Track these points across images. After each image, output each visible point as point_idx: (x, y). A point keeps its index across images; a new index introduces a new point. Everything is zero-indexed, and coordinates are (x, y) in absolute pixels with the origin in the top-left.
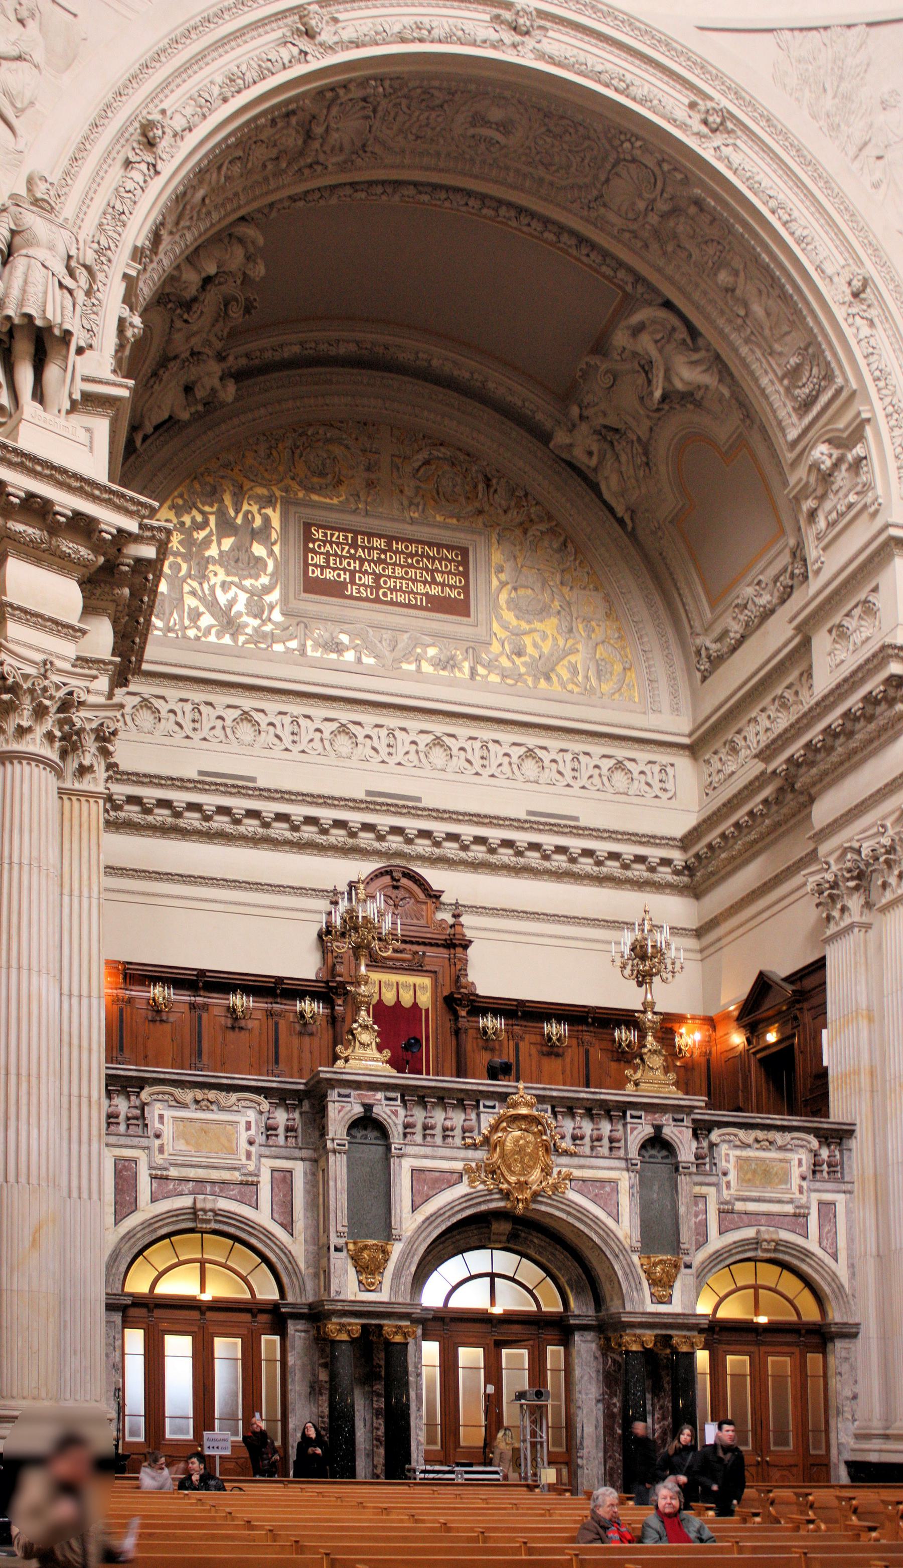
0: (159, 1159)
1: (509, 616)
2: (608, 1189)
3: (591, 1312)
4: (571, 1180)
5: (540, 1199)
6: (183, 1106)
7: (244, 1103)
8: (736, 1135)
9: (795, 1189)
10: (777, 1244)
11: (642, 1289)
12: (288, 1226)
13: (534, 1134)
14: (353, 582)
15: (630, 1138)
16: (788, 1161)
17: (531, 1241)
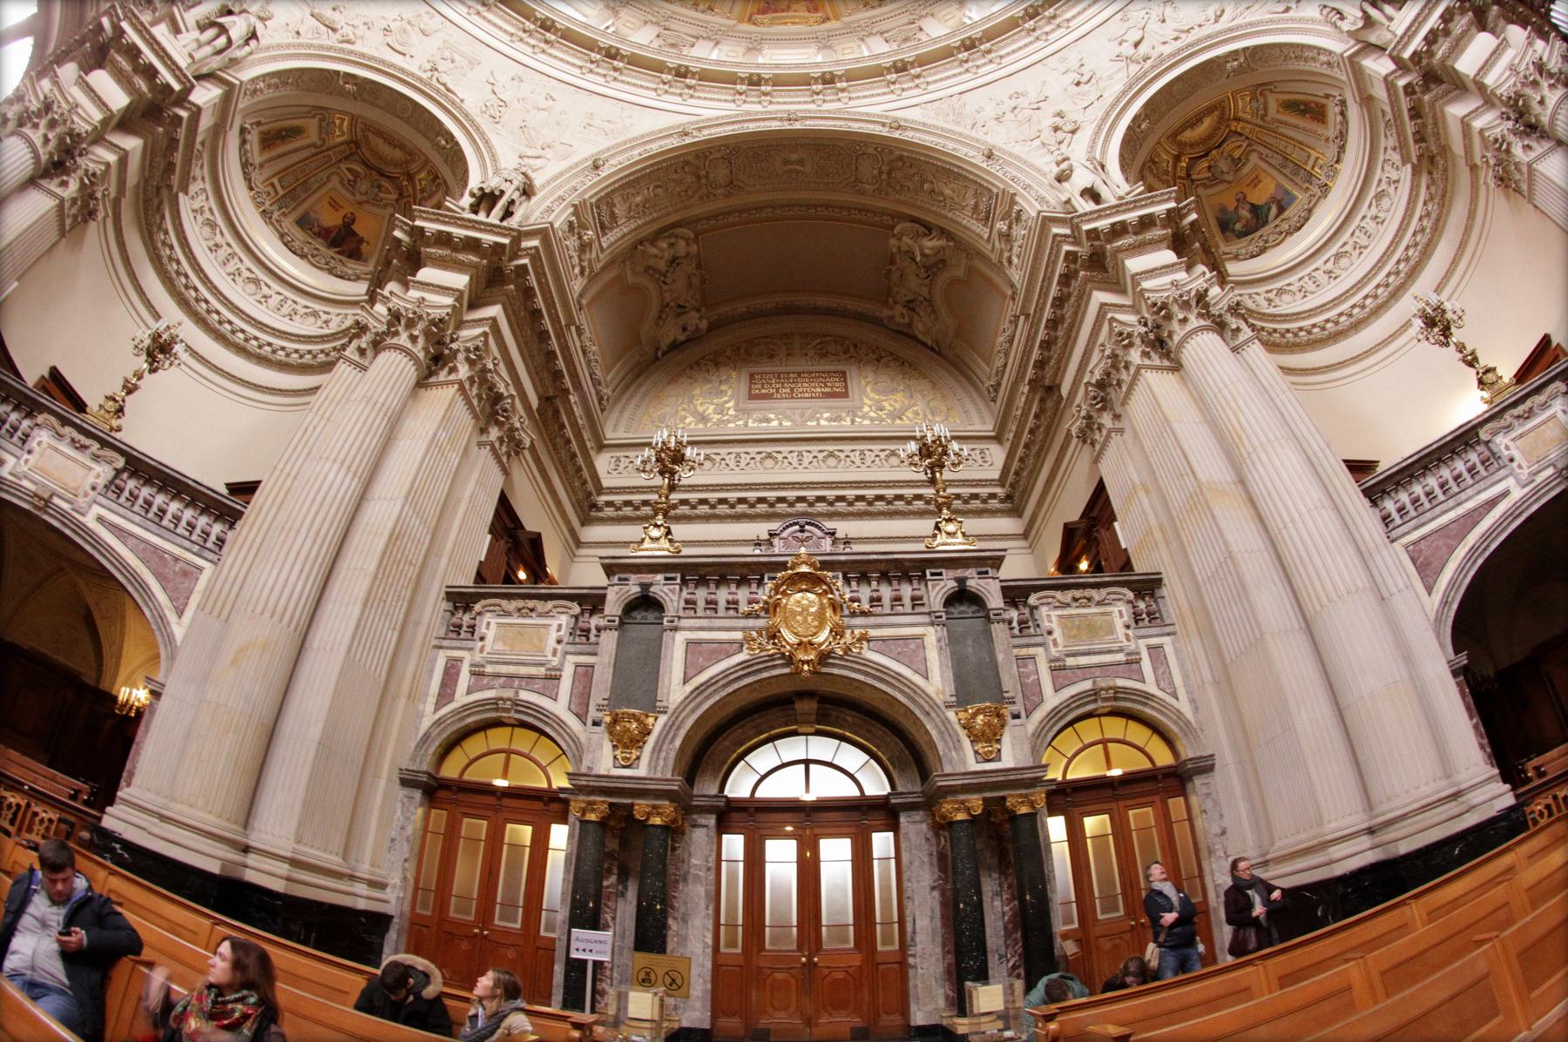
0: (478, 658)
1: (872, 395)
2: (912, 646)
3: (918, 788)
4: (868, 641)
5: (831, 661)
6: (508, 614)
7: (559, 610)
8: (1053, 597)
9: (1122, 637)
10: (1116, 692)
11: (961, 748)
12: (581, 717)
13: (819, 595)
14: (777, 392)
15: (932, 594)
16: (1109, 614)
17: (846, 721)
